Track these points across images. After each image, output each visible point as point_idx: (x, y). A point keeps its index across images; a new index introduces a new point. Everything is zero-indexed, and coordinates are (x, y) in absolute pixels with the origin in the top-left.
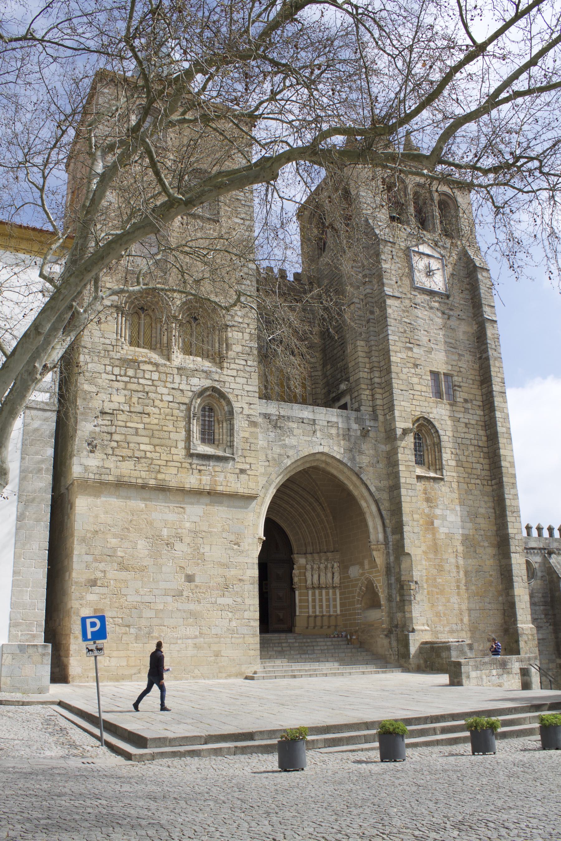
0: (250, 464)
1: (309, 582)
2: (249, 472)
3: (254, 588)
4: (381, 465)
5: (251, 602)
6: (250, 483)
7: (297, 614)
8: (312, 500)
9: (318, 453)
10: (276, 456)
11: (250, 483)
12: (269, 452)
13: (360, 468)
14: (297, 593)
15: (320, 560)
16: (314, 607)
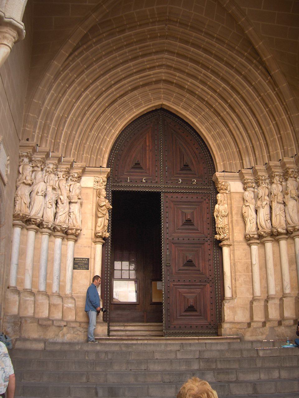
7: (228, 293)
14: (226, 250)
15: (271, 177)
16: (265, 278)
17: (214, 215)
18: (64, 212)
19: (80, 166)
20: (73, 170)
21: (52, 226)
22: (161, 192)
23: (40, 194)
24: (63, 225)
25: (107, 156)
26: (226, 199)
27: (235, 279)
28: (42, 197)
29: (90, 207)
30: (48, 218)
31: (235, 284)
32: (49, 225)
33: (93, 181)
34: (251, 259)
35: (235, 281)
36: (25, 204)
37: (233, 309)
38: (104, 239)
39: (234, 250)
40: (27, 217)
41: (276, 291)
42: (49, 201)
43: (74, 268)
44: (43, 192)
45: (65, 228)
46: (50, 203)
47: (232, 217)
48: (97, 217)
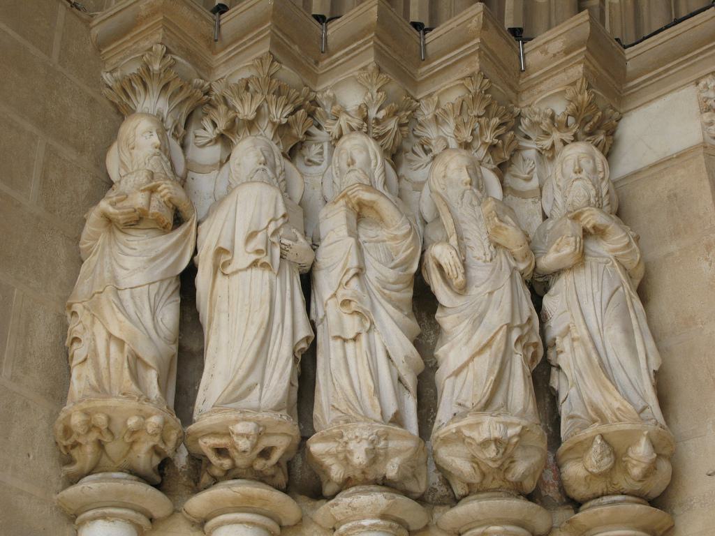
18: (480, 337)
19: (557, 46)
20: (535, 91)
21: (375, 456)
23: (242, 257)
24: (470, 426)
28: (261, 278)
30: (343, 407)
32: (351, 452)
33: (696, 108)
36: (121, 343)
40: (132, 422)
42: (344, 293)
44: (258, 243)
45: (496, 441)
46: (344, 310)
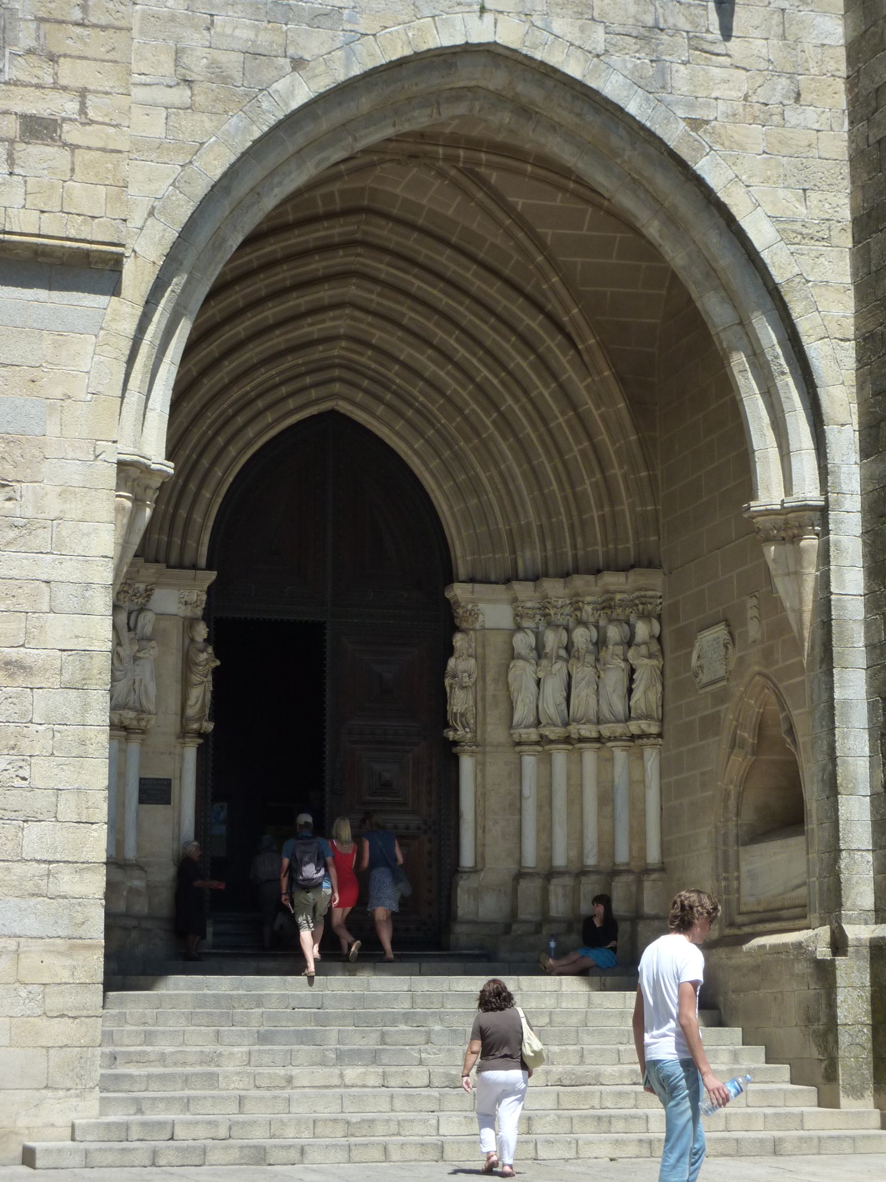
0: (83, 93)
1: (523, 712)
2: (71, 133)
3: (86, 707)
4: (810, 116)
5: (66, 777)
6: (76, 188)
7: (467, 859)
8: (533, 323)
9: (468, 50)
10: (232, 61)
11: (76, 188)
12: (195, 39)
13: (696, 124)
14: (467, 764)
16: (546, 829)
17: (444, 683)
19: (153, 571)
22: (325, 622)
25: (206, 539)
26: (473, 645)
27: (484, 828)
29: (173, 660)
31: (484, 838)
34: (521, 785)
35: (484, 832)
37: (477, 894)
38: (200, 734)
39: (484, 764)
41: (569, 860)
43: (141, 801)
47: (484, 689)
48: (186, 684)
